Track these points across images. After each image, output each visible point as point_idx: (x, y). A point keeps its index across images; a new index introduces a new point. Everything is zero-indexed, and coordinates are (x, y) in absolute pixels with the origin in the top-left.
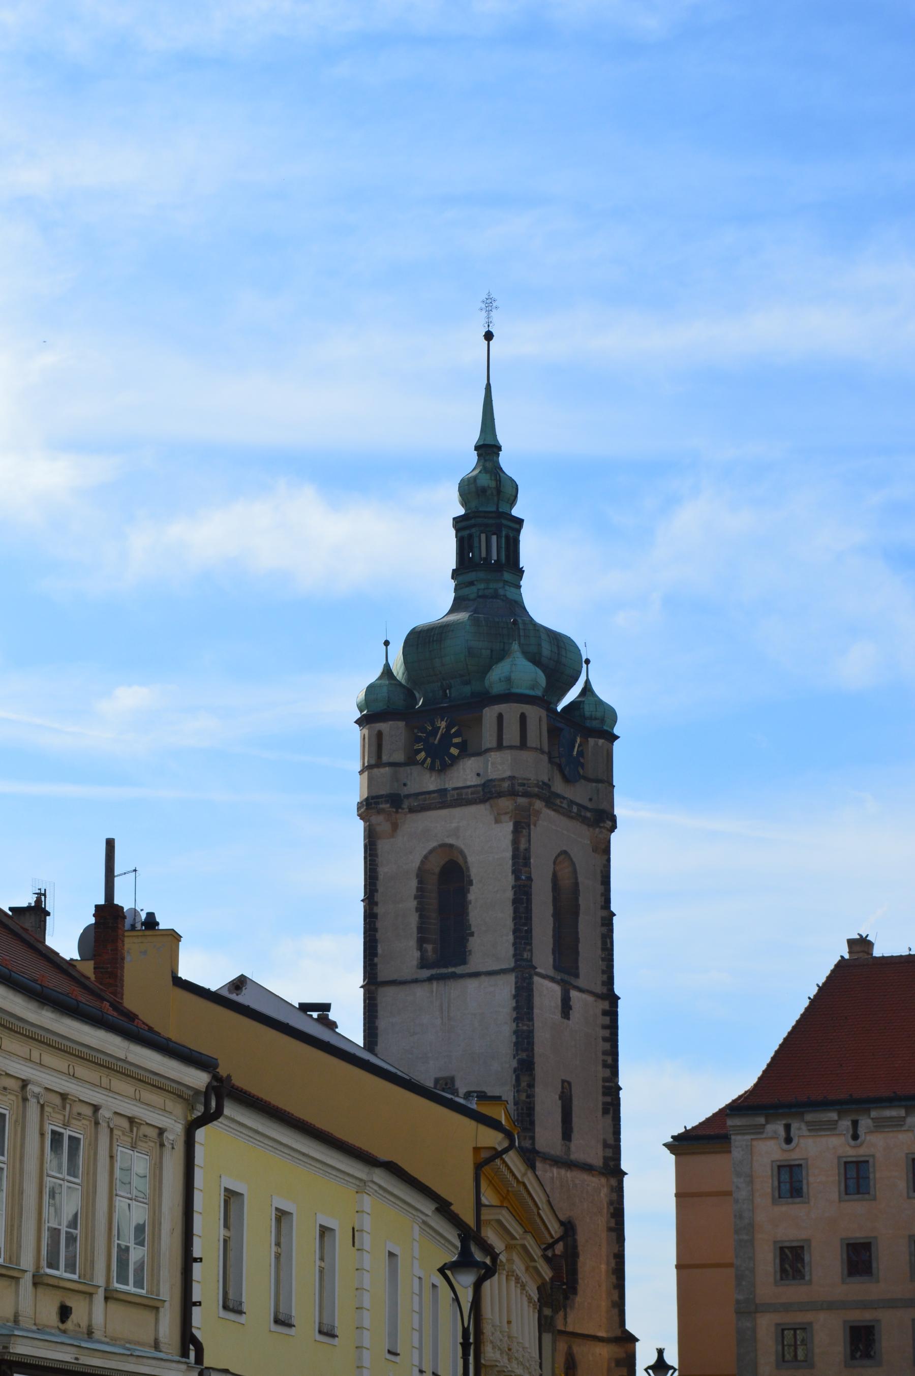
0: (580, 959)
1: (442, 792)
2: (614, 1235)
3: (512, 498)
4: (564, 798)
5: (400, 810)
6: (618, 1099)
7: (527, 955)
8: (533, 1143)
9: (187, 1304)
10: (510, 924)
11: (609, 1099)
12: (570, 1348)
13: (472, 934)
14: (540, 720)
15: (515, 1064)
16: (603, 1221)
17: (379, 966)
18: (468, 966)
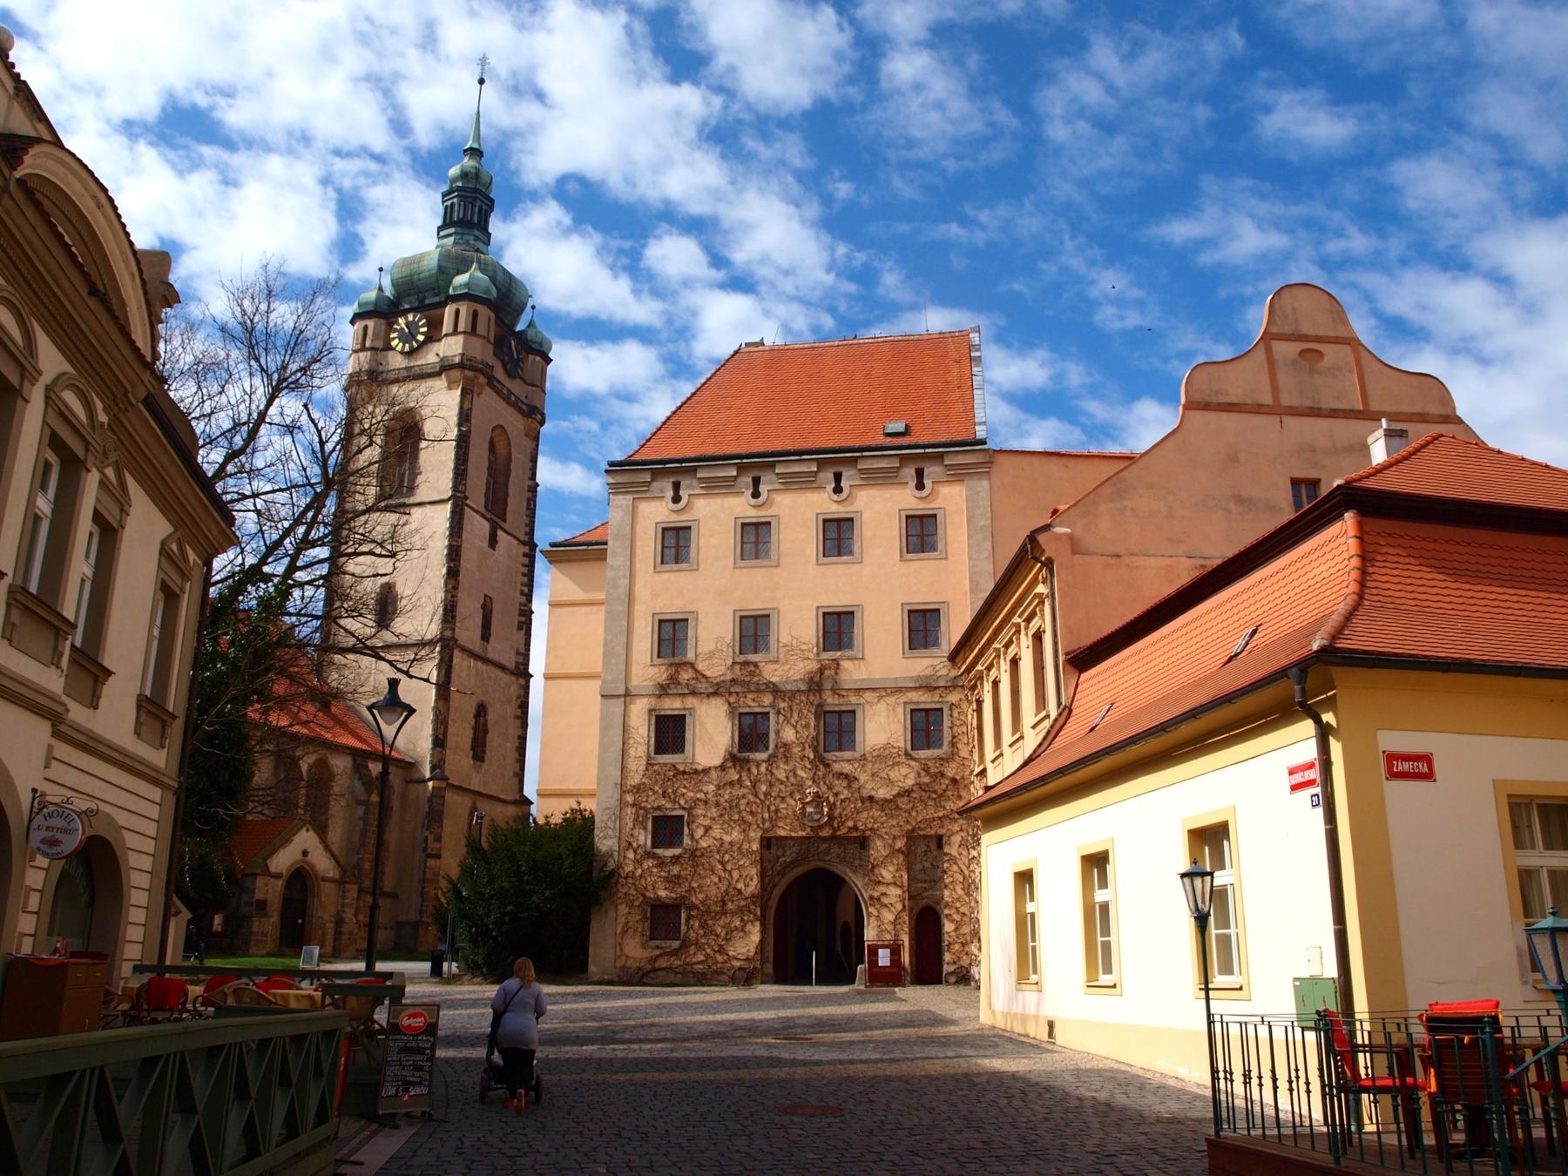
2: (519, 722)
6: (531, 620)
8: (453, 633)
10: (451, 465)
11: (523, 619)
12: (474, 803)
13: (420, 473)
14: (489, 319)
16: (512, 710)
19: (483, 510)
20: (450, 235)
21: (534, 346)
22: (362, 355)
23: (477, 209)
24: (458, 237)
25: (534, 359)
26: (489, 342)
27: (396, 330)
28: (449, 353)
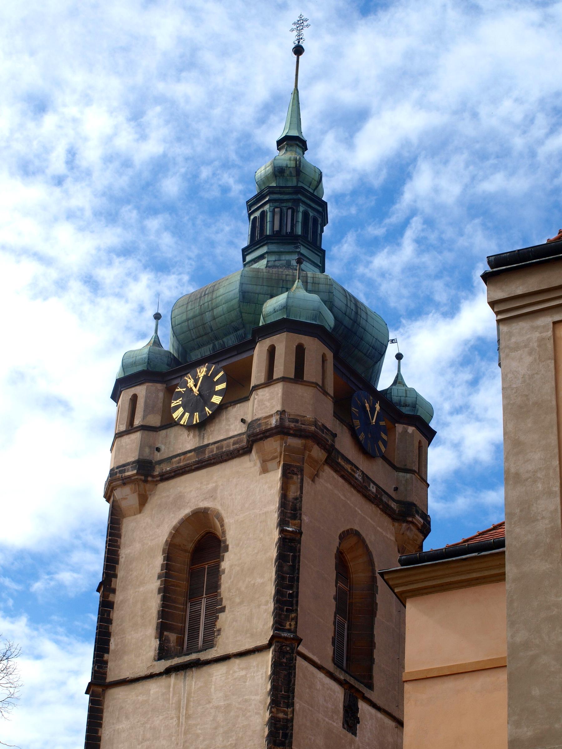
0: (375, 668)
3: (315, 183)
4: (358, 469)
5: (150, 479)
7: (290, 625)
10: (271, 589)
13: (223, 610)
17: (109, 664)
18: (216, 648)
19: (330, 666)
20: (261, 257)
21: (405, 410)
22: (126, 440)
23: (300, 215)
24: (273, 258)
25: (406, 431)
26: (325, 393)
27: (180, 395)
28: (260, 414)
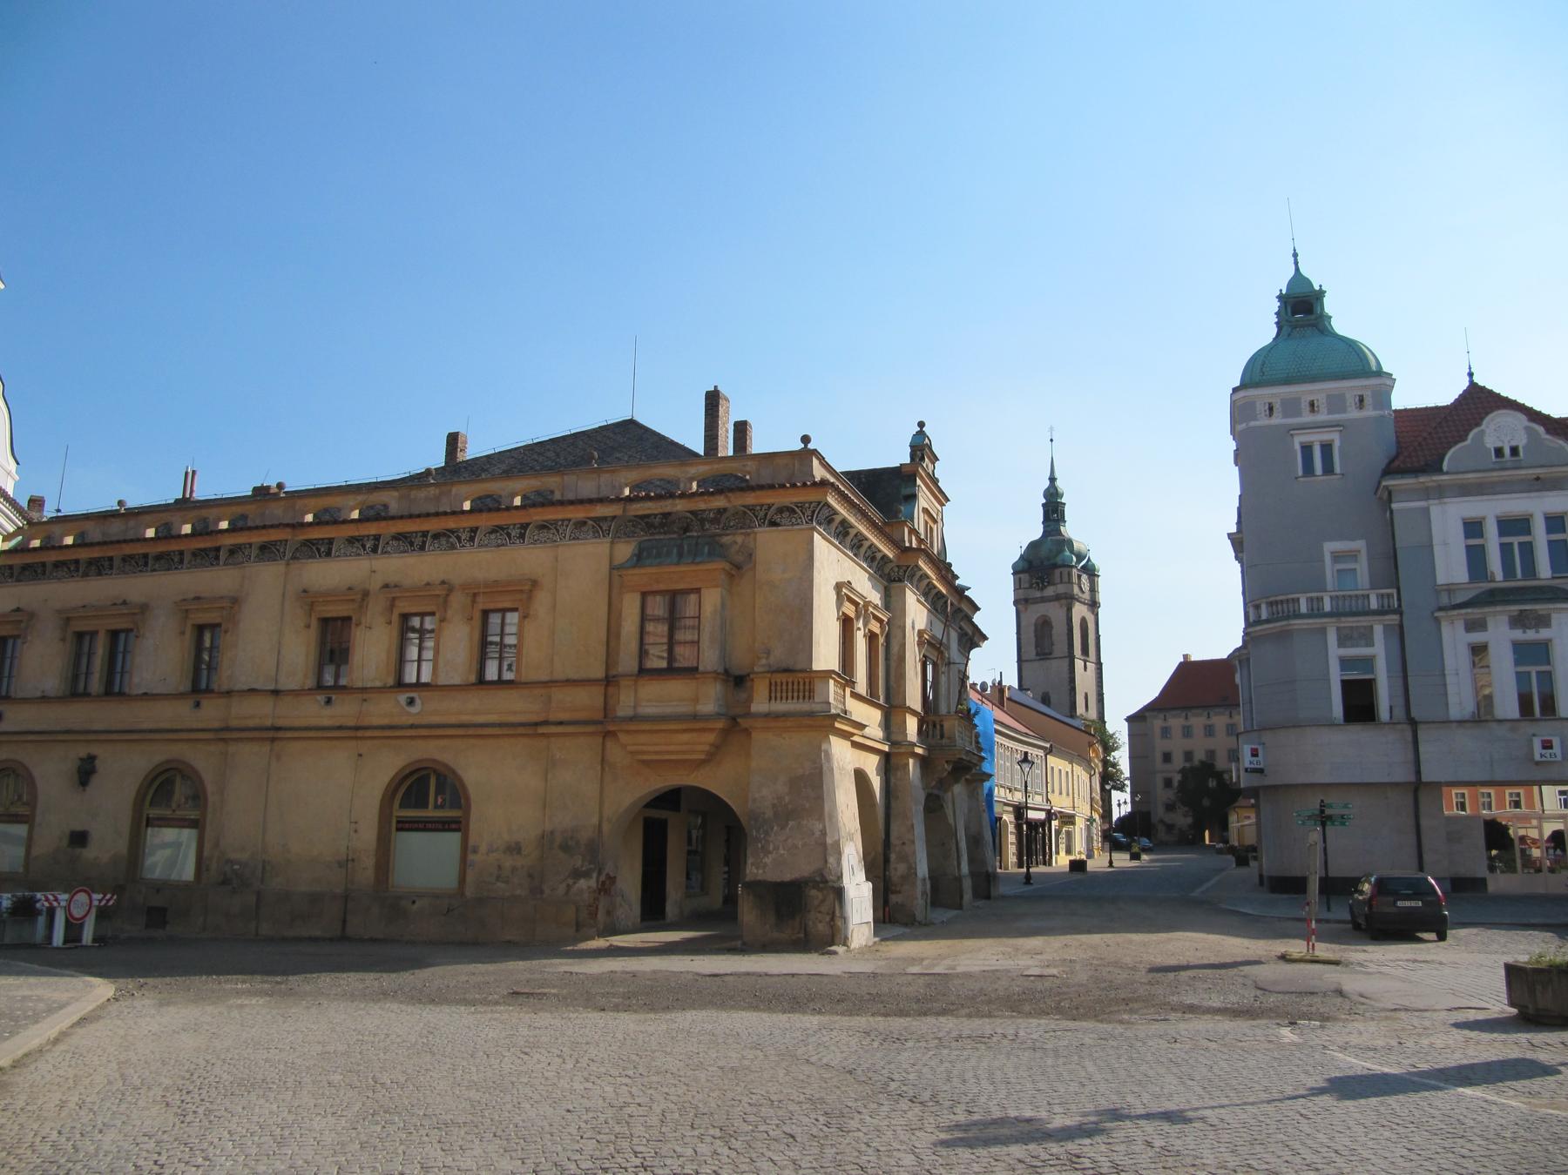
1: (1042, 597)
9: (1047, 792)
15: (1069, 687)
